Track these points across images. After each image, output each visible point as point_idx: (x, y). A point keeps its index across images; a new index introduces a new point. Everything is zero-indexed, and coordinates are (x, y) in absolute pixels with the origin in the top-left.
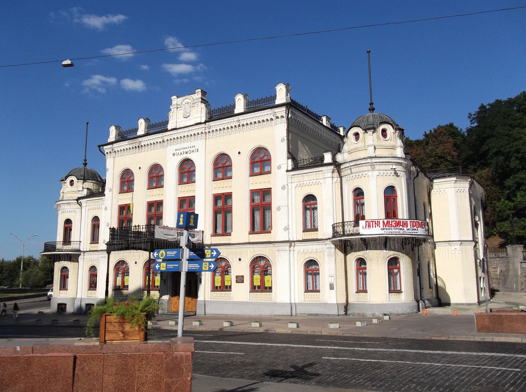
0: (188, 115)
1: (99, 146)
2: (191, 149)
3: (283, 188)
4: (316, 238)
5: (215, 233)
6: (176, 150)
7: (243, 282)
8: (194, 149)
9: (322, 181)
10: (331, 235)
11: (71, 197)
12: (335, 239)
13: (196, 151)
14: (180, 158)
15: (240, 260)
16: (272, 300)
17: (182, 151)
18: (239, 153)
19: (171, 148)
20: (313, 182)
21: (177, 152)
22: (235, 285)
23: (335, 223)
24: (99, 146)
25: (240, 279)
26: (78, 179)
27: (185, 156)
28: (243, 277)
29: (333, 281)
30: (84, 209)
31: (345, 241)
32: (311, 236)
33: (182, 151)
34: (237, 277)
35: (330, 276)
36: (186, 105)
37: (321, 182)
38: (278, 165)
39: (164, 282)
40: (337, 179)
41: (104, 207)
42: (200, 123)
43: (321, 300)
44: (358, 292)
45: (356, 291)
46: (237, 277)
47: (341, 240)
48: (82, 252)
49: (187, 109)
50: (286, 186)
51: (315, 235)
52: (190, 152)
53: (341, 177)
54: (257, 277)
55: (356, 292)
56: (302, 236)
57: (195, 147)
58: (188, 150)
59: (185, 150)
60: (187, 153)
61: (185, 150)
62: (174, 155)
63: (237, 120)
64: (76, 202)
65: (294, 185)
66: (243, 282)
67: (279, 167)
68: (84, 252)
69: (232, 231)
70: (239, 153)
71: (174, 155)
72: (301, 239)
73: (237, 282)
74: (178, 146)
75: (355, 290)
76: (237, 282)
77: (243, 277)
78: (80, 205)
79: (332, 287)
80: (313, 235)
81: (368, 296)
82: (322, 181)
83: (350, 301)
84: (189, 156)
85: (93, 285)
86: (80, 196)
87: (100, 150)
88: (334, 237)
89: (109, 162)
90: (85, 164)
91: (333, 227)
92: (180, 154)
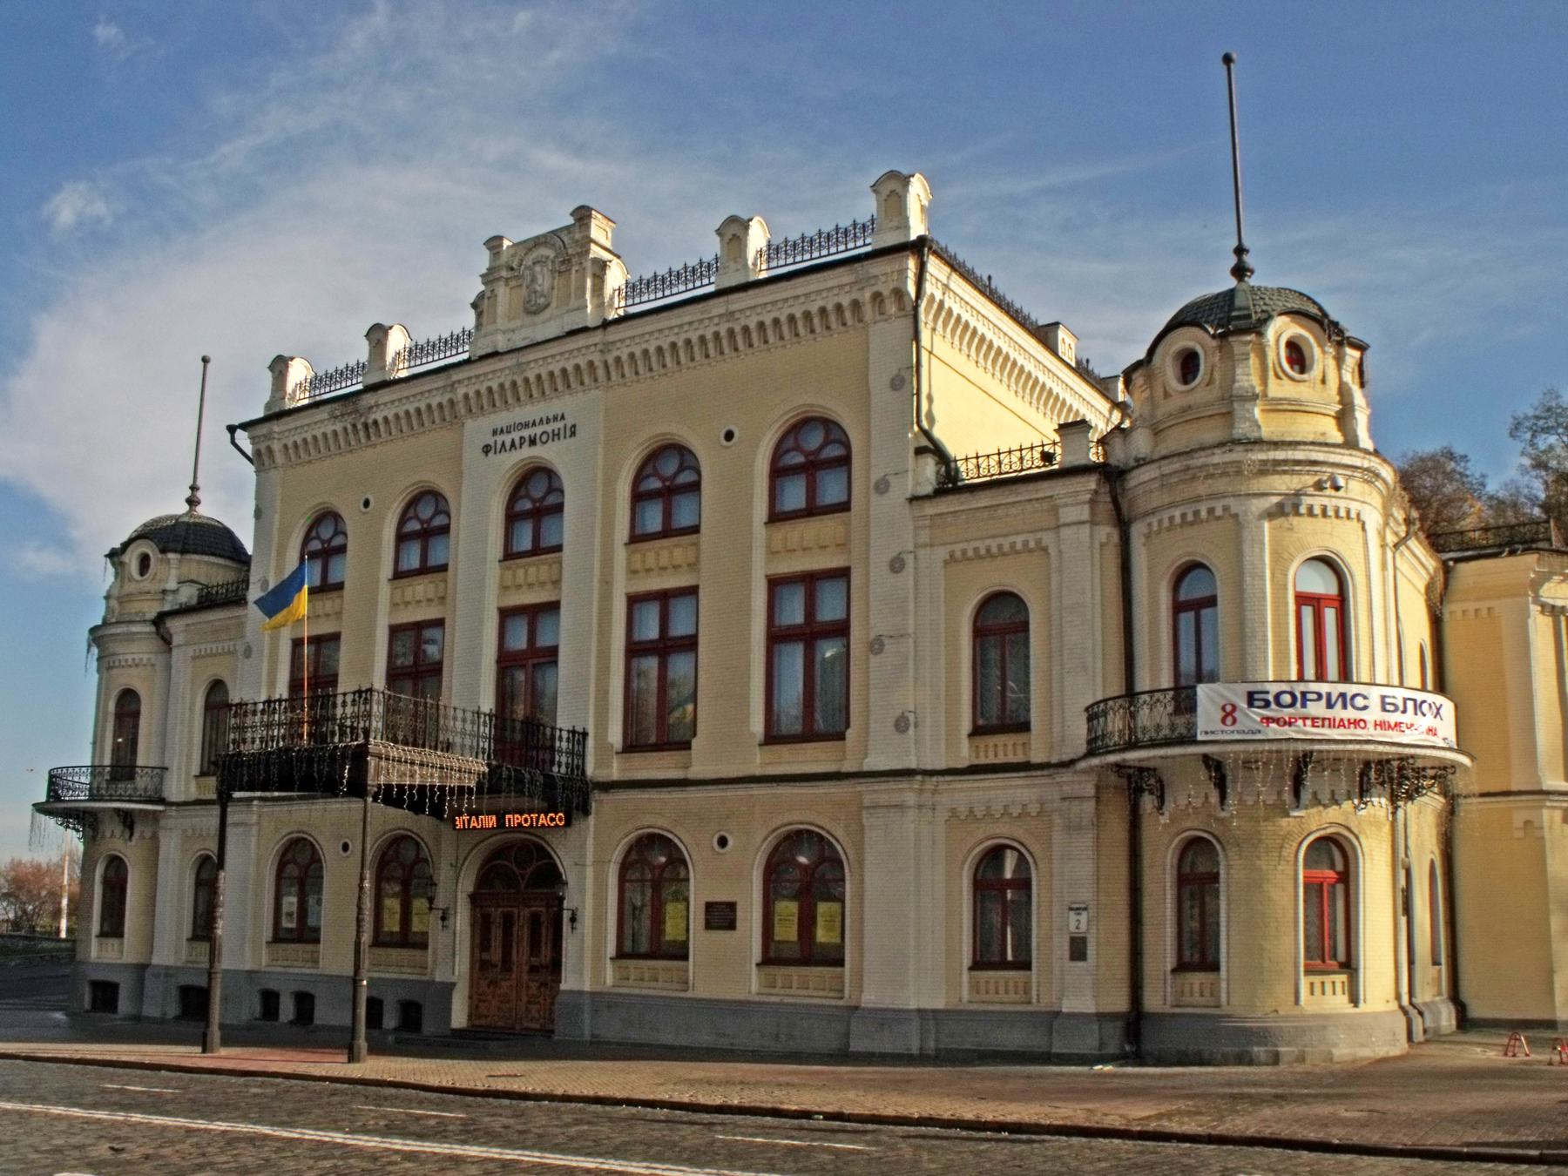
0: (542, 301)
1: (232, 429)
2: (549, 428)
3: (897, 565)
4: (1020, 758)
5: (632, 745)
6: (495, 433)
7: (731, 925)
8: (560, 424)
9: (1047, 538)
11: (137, 614)
12: (1095, 761)
13: (568, 433)
14: (509, 463)
15: (723, 842)
16: (842, 998)
17: (516, 435)
18: (729, 436)
19: (478, 429)
20: (1013, 545)
21: (500, 439)
22: (701, 940)
23: (1100, 697)
24: (232, 429)
25: (721, 916)
26: (163, 551)
27: (527, 452)
28: (732, 906)
29: (1083, 927)
30: (176, 654)
31: (1141, 770)
32: (1001, 754)
33: (516, 435)
34: (710, 907)
35: (1071, 909)
36: (538, 268)
37: (1044, 544)
38: (875, 476)
39: (443, 918)
40: (1107, 532)
41: (240, 648)
42: (585, 330)
43: (1034, 1001)
44: (1182, 967)
45: (1175, 965)
47: (1119, 767)
48: (172, 804)
49: (540, 281)
50: (909, 559)
51: (1020, 749)
52: (544, 438)
53: (1123, 524)
54: (788, 909)
55: (1174, 971)
56: (965, 754)
57: (563, 417)
58: (538, 430)
59: (526, 433)
60: (533, 442)
61: (526, 433)
63: (721, 310)
64: (153, 629)
65: (942, 553)
66: (731, 925)
67: (882, 487)
68: (178, 804)
69: (695, 734)
70: (729, 436)
71: (487, 449)
72: (962, 764)
73: (709, 926)
74: (502, 418)
75: (1170, 962)
76: (709, 926)
77: (732, 906)
78: (166, 641)
79: (1078, 950)
80: (1010, 748)
81: (1224, 985)
82: (1047, 538)
83: (1154, 1001)
85: (204, 927)
86: (167, 608)
87: (233, 442)
88: (1091, 753)
90: (192, 502)
91: (1090, 719)
92: (508, 447)
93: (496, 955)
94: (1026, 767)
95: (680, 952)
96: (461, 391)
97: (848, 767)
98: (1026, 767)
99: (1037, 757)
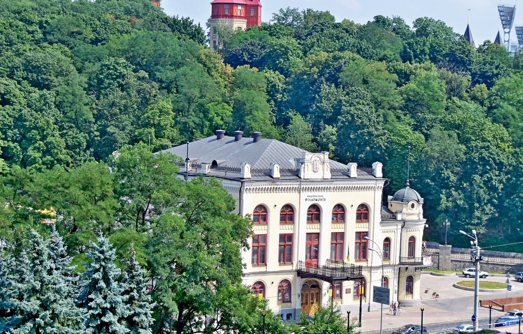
2: (320, 198)
9: (396, 230)
10: (398, 262)
17: (313, 198)
19: (305, 195)
21: (309, 198)
27: (314, 202)
34: (346, 289)
46: (346, 289)
58: (318, 198)
60: (316, 200)
62: (306, 200)
71: (306, 200)
73: (346, 293)
84: (317, 202)
89: (246, 196)
93: (304, 302)
94: (389, 266)
95: (341, 296)
96: (302, 186)
97: (369, 265)
98: (389, 266)
99: (391, 264)
